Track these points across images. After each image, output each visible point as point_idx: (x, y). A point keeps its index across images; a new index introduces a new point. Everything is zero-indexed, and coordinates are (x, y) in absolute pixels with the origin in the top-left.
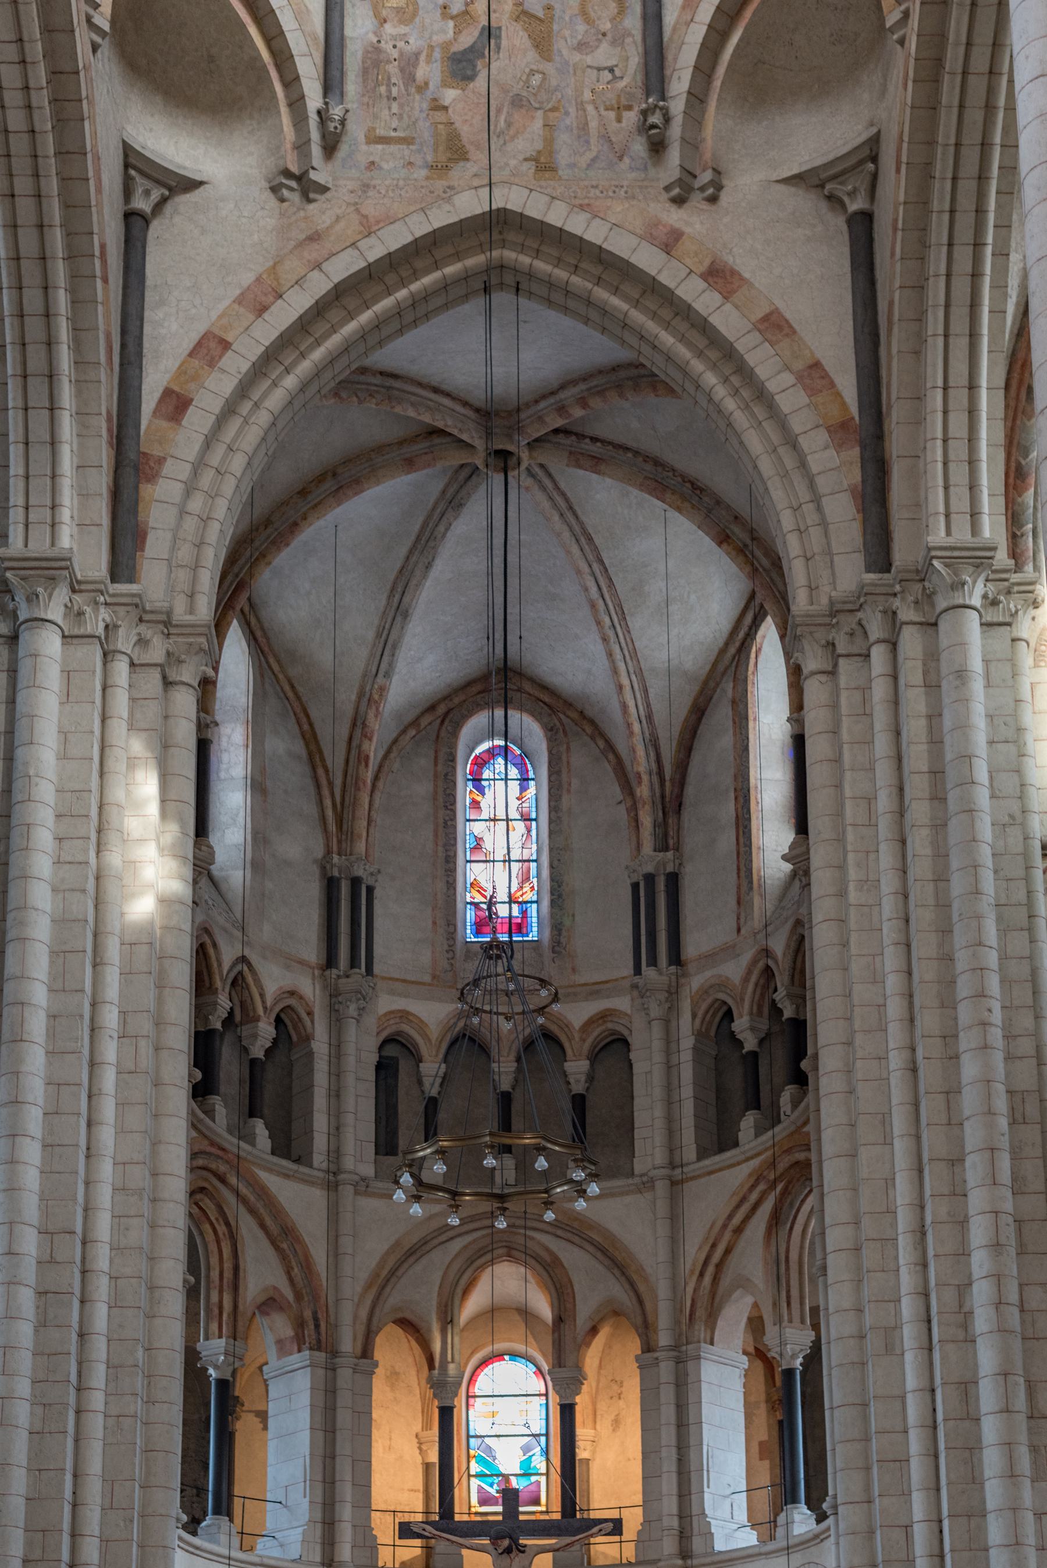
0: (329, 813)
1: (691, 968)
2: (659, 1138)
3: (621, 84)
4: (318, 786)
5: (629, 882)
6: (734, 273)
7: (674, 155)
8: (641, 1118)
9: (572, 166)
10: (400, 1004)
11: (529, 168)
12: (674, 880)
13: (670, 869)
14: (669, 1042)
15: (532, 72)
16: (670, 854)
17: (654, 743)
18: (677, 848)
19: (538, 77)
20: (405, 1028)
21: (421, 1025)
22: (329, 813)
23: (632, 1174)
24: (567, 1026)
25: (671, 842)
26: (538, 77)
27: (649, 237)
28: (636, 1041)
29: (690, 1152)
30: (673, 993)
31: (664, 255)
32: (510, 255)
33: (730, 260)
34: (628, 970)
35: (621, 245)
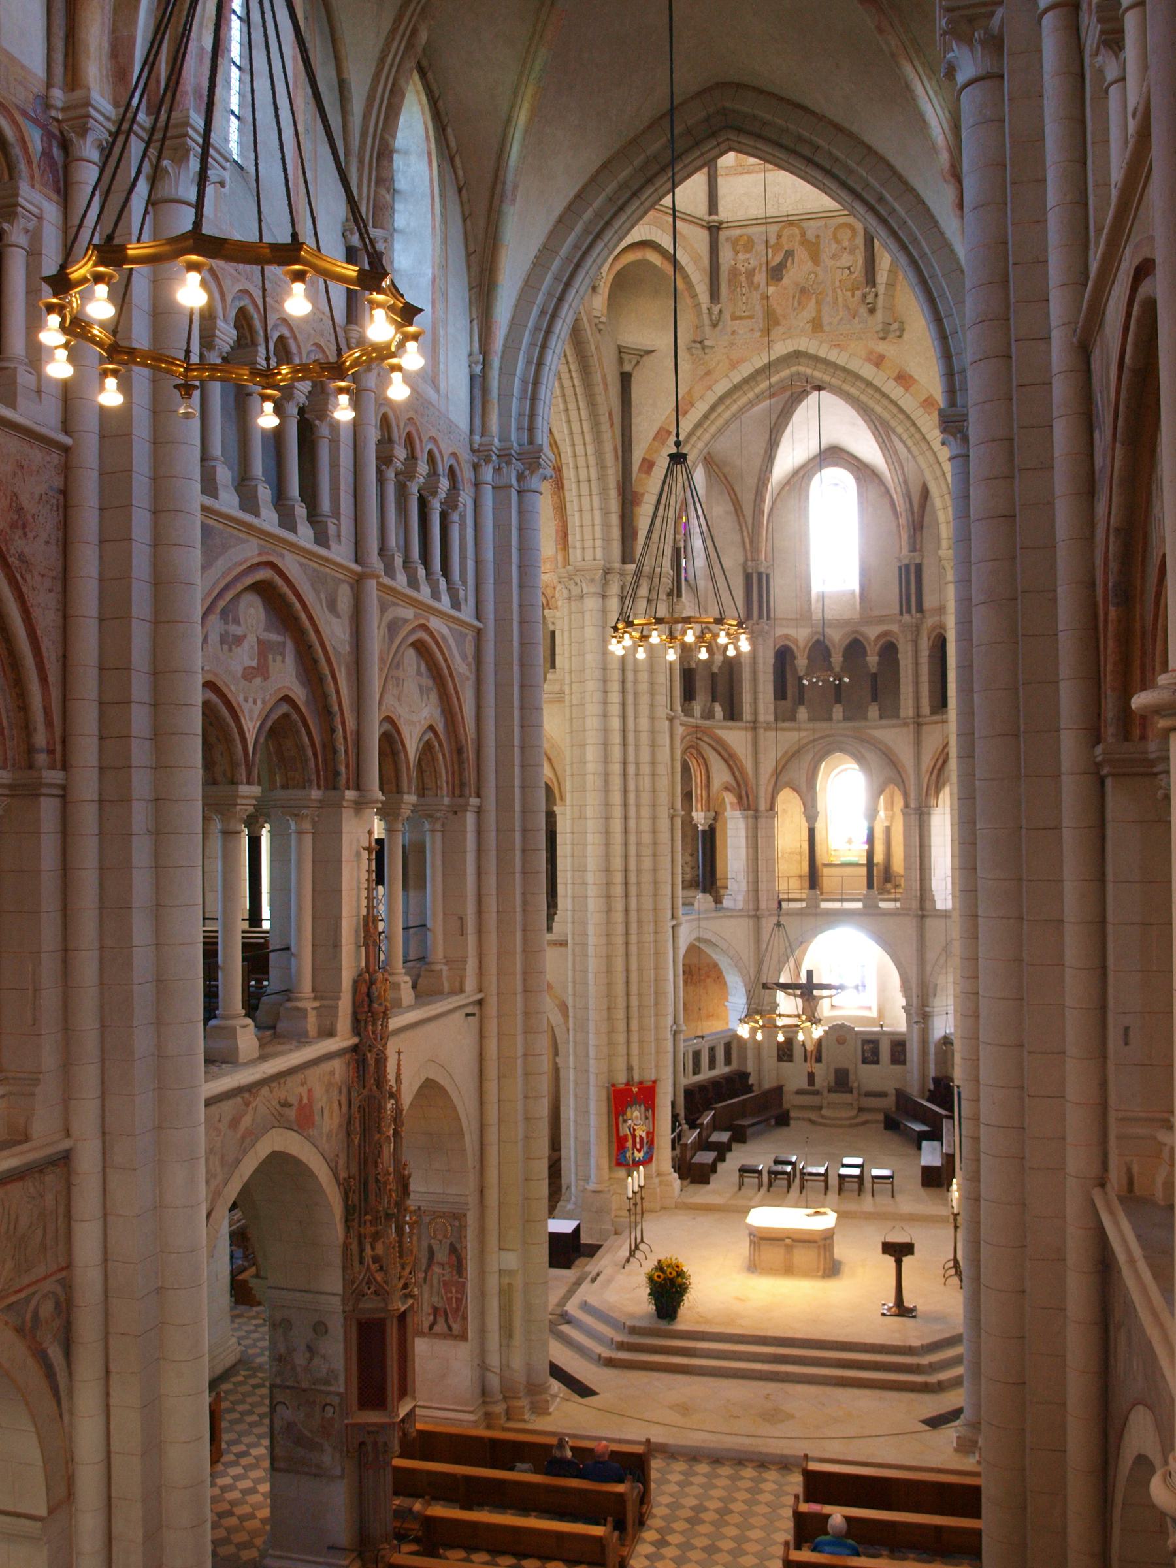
0: (747, 540)
1: (927, 614)
2: (910, 703)
3: (854, 276)
4: (740, 525)
5: (898, 564)
6: (911, 377)
7: (879, 314)
8: (903, 689)
9: (830, 324)
10: (786, 631)
11: (809, 327)
12: (919, 568)
13: (917, 561)
14: (916, 652)
15: (810, 273)
16: (916, 554)
17: (908, 495)
18: (921, 550)
19: (813, 276)
20: (787, 642)
21: (796, 641)
22: (747, 540)
23: (898, 717)
24: (867, 639)
25: (918, 547)
26: (813, 276)
27: (869, 360)
28: (901, 647)
29: (926, 709)
30: (918, 628)
31: (875, 369)
32: (802, 369)
33: (908, 369)
34: (897, 611)
35: (855, 365)
